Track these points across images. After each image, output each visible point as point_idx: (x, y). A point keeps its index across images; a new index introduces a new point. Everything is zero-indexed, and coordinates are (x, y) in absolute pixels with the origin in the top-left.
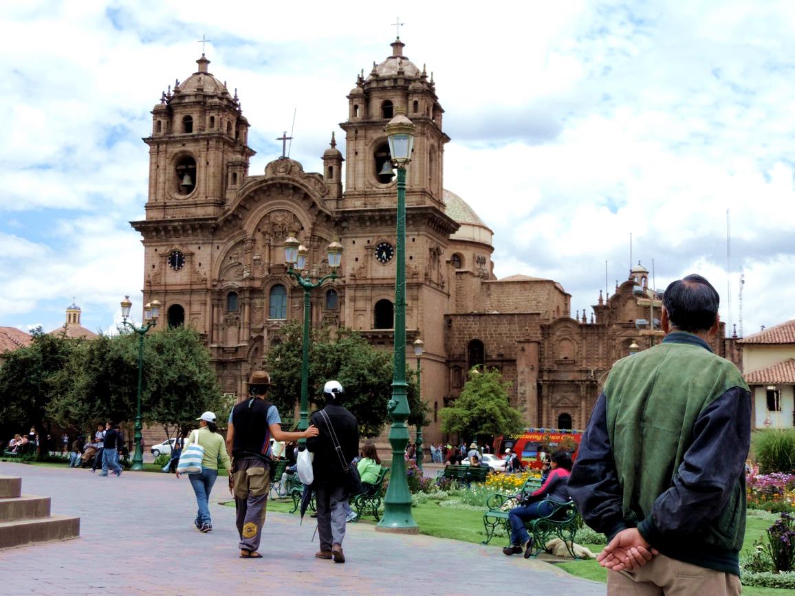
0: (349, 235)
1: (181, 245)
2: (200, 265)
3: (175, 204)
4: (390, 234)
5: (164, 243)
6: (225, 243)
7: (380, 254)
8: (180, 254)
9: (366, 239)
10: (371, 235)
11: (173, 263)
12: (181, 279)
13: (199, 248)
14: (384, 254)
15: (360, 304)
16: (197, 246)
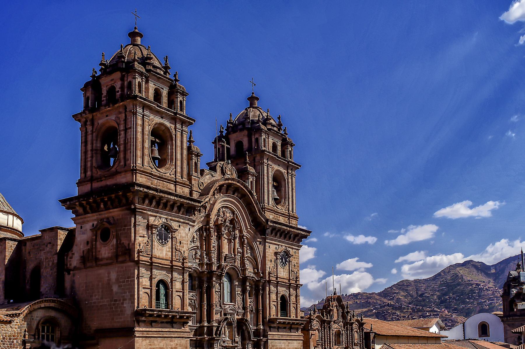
0: (268, 241)
1: (166, 219)
2: (180, 242)
3: (158, 175)
4: (287, 245)
5: (154, 214)
6: (194, 226)
7: (282, 259)
8: (168, 228)
9: (275, 246)
10: (278, 243)
11: (160, 235)
12: (166, 254)
13: (180, 227)
14: (284, 260)
15: (273, 296)
16: (177, 224)
